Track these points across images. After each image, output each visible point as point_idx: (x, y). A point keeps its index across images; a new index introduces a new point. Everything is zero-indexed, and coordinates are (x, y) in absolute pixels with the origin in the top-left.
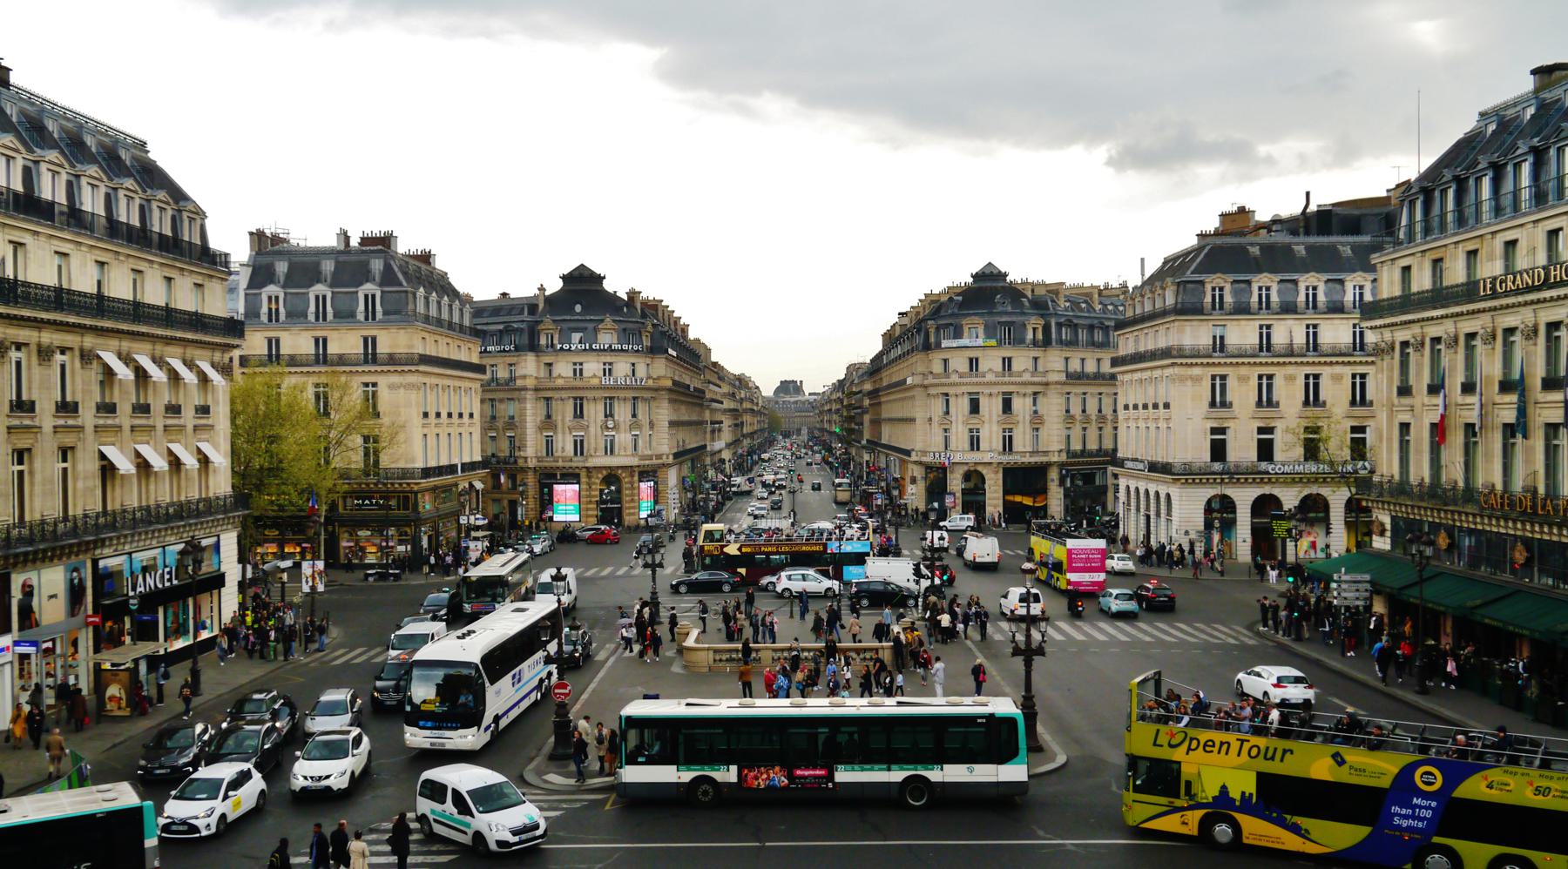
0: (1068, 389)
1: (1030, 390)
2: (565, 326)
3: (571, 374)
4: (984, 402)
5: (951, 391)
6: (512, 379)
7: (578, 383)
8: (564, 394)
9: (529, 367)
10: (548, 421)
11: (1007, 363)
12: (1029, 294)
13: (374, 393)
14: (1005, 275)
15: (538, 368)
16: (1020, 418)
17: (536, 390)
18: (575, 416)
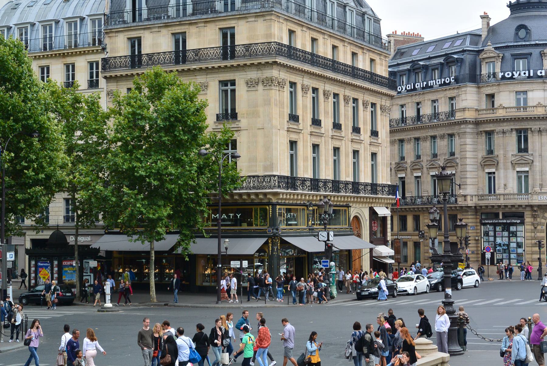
2: (508, 54)
3: (514, 104)
6: (452, 113)
7: (522, 114)
8: (506, 127)
9: (469, 99)
10: (490, 158)
13: (233, 91)
15: (479, 100)
17: (477, 123)
18: (520, 150)
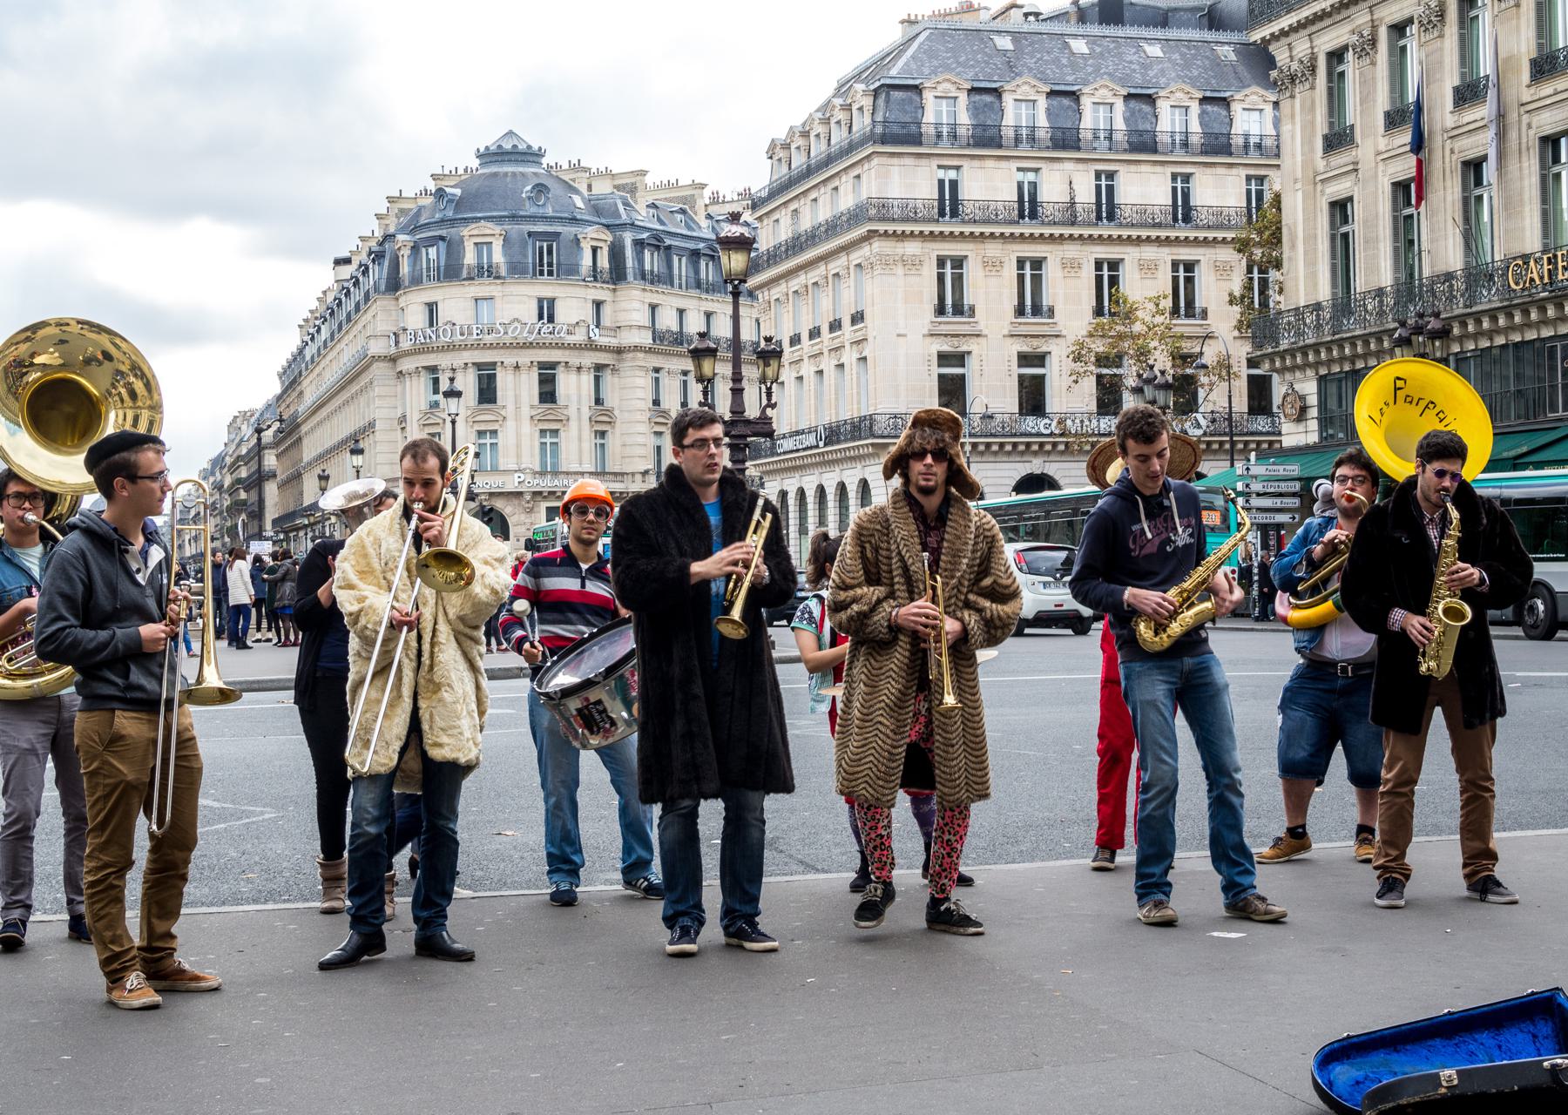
0: (656, 361)
1: (589, 359)
4: (504, 381)
5: (443, 361)
11: (546, 310)
12: (583, 189)
14: (539, 154)
16: (572, 412)
